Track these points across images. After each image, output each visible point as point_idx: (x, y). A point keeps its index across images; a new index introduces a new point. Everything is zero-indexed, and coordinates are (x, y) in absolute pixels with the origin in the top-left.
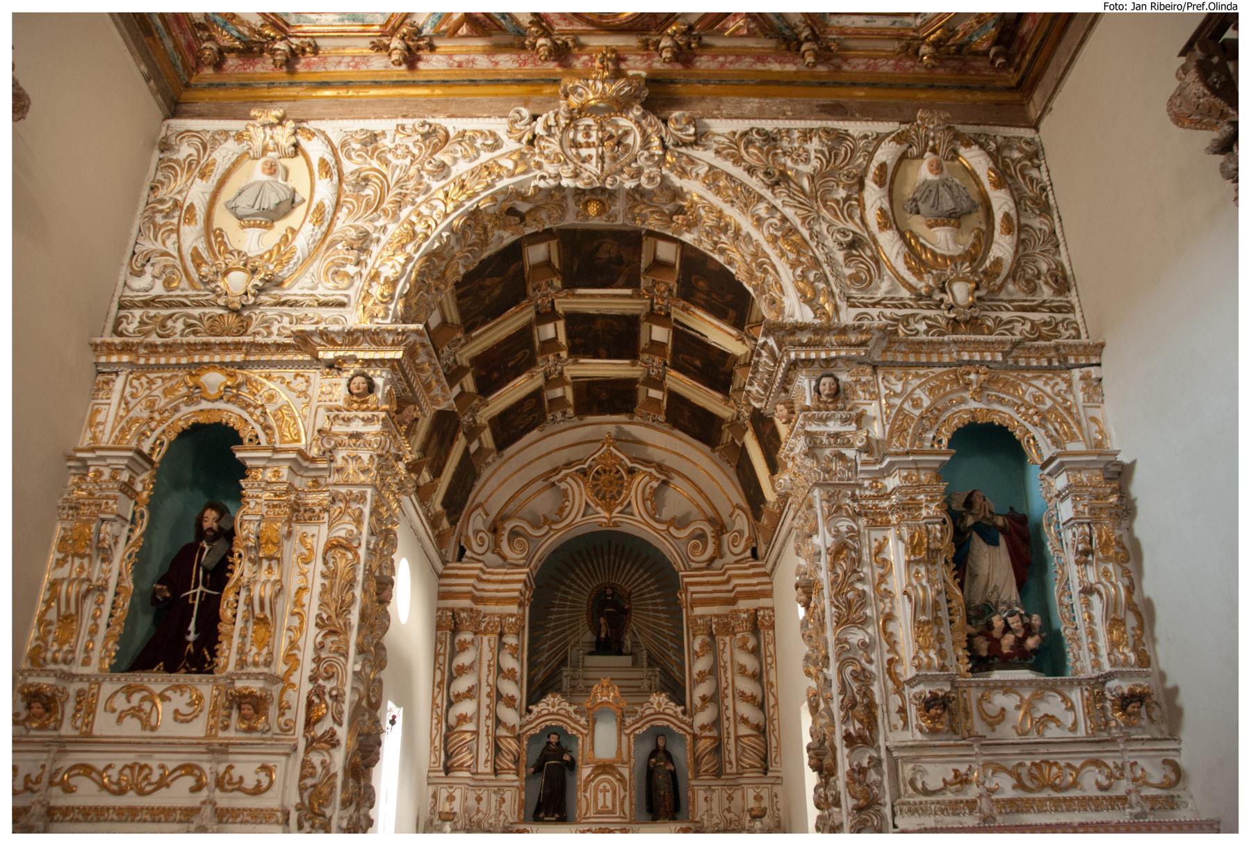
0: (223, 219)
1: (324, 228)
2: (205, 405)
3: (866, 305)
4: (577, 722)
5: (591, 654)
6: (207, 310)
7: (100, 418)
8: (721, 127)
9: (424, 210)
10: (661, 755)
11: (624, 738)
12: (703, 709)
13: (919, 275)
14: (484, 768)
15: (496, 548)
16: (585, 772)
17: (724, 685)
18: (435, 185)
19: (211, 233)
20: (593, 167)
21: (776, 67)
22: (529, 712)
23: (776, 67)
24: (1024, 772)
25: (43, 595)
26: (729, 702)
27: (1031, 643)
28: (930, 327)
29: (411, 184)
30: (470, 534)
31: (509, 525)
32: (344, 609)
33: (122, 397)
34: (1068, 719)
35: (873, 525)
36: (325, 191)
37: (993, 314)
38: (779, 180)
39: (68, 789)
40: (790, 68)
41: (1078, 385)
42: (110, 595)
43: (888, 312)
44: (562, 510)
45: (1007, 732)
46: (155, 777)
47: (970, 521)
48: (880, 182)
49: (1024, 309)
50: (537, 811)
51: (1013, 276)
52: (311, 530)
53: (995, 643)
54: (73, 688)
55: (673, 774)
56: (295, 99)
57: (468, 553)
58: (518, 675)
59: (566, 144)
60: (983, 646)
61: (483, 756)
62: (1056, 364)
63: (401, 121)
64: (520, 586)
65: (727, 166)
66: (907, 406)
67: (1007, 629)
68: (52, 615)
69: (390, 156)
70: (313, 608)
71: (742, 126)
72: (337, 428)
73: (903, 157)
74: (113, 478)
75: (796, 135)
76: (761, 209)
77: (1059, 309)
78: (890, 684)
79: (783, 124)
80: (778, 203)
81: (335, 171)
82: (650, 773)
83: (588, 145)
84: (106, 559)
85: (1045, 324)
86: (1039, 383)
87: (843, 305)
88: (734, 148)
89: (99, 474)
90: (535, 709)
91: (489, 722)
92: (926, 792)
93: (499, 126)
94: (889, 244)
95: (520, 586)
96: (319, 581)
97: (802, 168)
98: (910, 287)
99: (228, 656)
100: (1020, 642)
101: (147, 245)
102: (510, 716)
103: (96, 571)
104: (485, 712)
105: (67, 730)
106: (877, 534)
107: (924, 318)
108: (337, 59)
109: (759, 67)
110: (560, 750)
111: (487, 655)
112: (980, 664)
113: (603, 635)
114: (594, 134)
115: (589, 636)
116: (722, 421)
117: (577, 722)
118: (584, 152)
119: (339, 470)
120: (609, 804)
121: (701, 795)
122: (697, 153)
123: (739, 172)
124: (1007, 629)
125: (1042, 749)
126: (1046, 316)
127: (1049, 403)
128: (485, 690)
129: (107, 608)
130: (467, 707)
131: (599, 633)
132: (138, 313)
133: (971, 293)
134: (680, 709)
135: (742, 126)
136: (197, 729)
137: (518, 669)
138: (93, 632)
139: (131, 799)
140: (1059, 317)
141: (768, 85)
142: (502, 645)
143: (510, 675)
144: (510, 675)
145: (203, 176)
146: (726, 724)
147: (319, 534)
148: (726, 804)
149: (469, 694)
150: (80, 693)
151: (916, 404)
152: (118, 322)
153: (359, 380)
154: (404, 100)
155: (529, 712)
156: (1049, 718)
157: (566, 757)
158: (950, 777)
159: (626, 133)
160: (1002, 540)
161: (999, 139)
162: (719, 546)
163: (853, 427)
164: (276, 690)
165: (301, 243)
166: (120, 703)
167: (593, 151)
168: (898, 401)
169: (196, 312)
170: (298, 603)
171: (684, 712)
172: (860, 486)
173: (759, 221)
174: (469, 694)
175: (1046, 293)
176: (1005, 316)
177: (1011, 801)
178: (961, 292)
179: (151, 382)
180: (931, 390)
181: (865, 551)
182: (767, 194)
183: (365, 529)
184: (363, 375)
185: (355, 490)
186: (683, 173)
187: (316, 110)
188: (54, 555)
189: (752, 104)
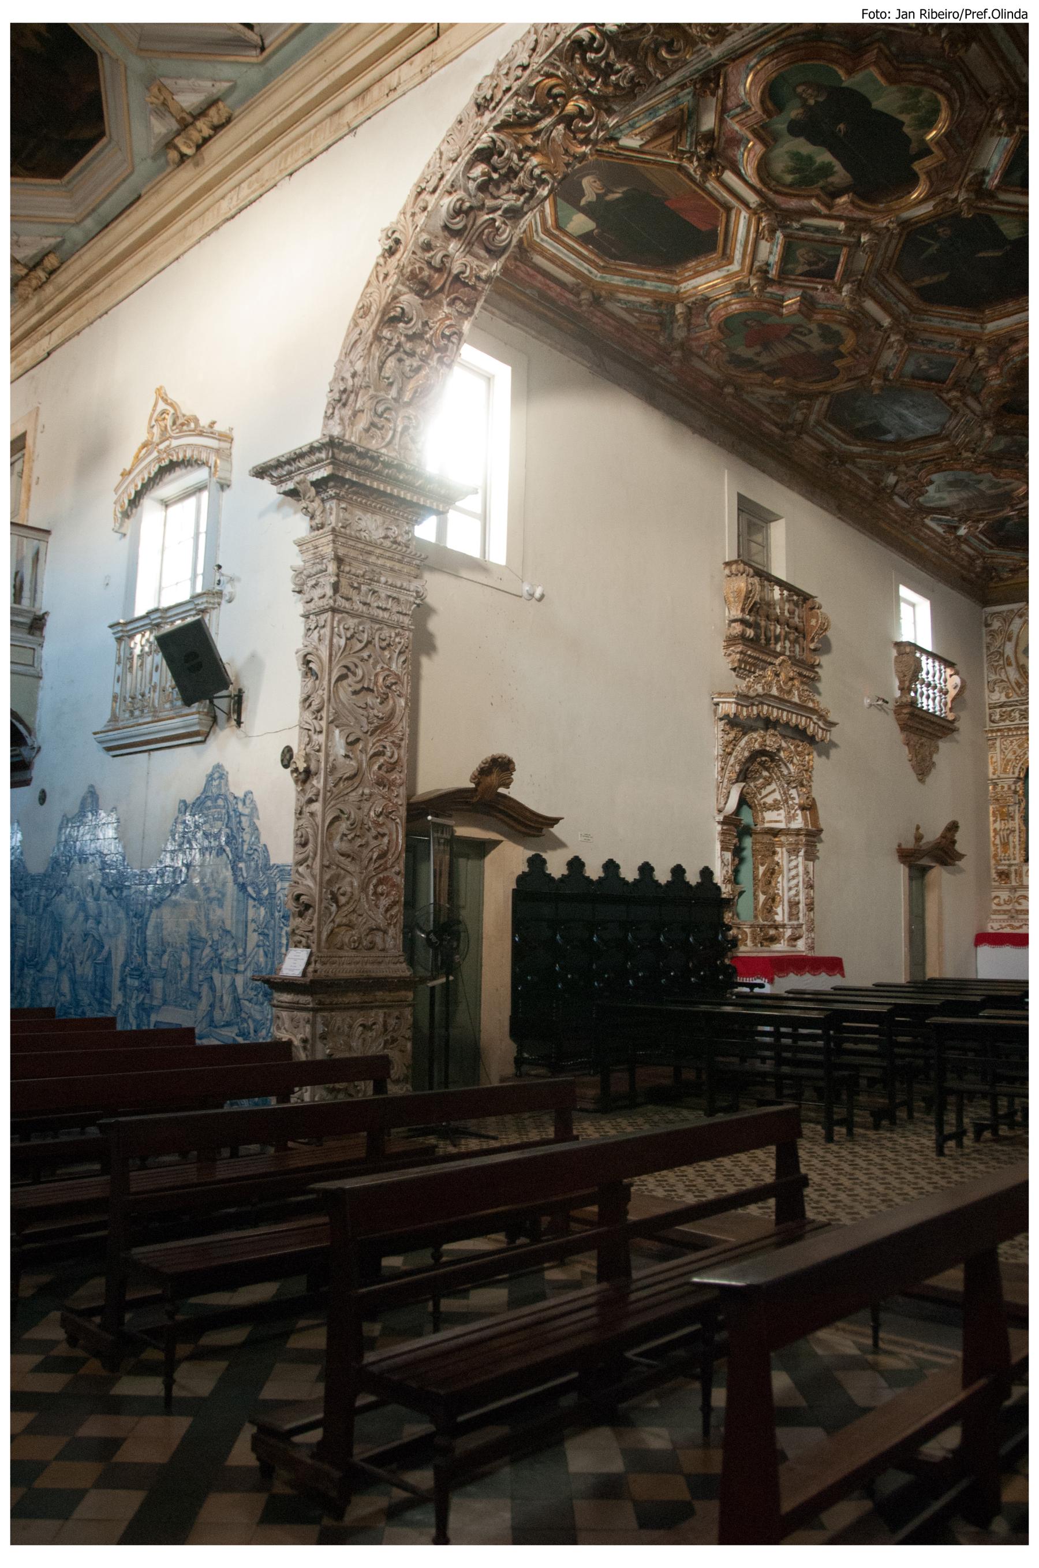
25: (992, 834)
39: (1020, 904)
54: (1013, 868)
68: (998, 841)
74: (1009, 788)
84: (1013, 820)
89: (1003, 787)
103: (1011, 824)
105: (1014, 884)
129: (1017, 838)
138: (1014, 847)
150: (1016, 871)
188: (992, 819)
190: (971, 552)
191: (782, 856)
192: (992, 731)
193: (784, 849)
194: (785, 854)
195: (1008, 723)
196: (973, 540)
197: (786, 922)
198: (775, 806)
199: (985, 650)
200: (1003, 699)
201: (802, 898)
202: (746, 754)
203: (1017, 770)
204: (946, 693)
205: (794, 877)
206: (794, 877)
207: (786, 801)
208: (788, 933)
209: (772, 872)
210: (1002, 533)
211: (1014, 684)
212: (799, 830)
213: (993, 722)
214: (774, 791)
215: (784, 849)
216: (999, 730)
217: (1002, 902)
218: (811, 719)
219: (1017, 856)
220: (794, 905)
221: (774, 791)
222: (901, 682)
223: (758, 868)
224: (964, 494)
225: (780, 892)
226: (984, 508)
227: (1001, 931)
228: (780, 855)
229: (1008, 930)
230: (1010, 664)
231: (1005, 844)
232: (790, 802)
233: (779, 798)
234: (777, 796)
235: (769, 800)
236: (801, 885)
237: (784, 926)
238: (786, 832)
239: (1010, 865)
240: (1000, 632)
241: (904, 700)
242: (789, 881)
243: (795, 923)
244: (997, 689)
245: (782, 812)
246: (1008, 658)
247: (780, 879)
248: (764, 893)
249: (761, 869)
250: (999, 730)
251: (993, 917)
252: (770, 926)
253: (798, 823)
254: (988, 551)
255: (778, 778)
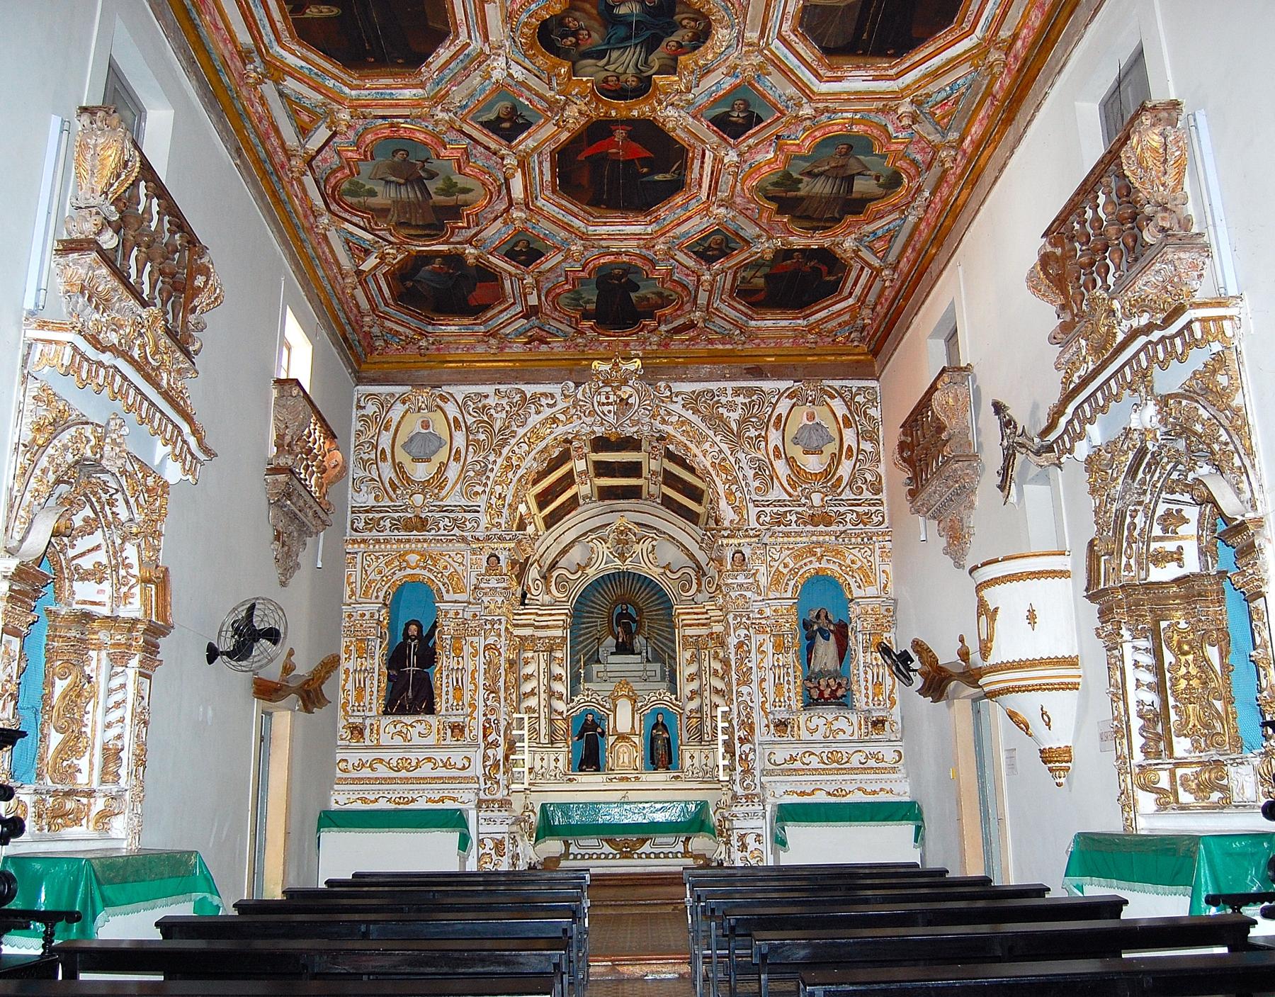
0: (402, 456)
1: (462, 463)
2: (409, 571)
3: (764, 506)
4: (604, 707)
5: (612, 654)
6: (402, 514)
7: (352, 579)
8: (687, 387)
9: (516, 448)
10: (660, 727)
11: (637, 717)
12: (691, 699)
13: (794, 488)
14: (545, 740)
15: (548, 592)
16: (611, 739)
17: (704, 682)
18: (521, 432)
19: (398, 467)
20: (611, 418)
21: (721, 347)
22: (572, 701)
23: (721, 347)
24: (824, 755)
26: (707, 694)
27: (839, 693)
28: (799, 518)
29: (507, 432)
30: (530, 583)
31: (555, 574)
32: (495, 680)
33: (363, 567)
34: (849, 730)
35: (758, 632)
36: (460, 440)
37: (835, 509)
38: (718, 423)
40: (729, 347)
41: (878, 552)
42: (376, 675)
43: (775, 509)
44: (591, 559)
45: (818, 736)
46: (414, 763)
47: (816, 627)
48: (777, 425)
49: (853, 505)
50: (581, 765)
51: (850, 484)
52: (475, 639)
53: (821, 694)
54: (368, 722)
55: (668, 740)
56: (431, 368)
57: (529, 596)
58: (564, 678)
59: (596, 404)
60: (815, 694)
61: (543, 732)
62: (866, 540)
63: (497, 387)
64: (563, 617)
65: (689, 414)
66: (781, 568)
67: (828, 685)
69: (492, 411)
70: (481, 681)
71: (699, 387)
72: (482, 585)
73: (794, 405)
74: (372, 615)
75: (729, 392)
76: (707, 446)
77: (874, 505)
78: (762, 713)
79: (722, 384)
80: (718, 439)
81: (463, 425)
82: (653, 740)
83: (608, 404)
84: (373, 658)
85: (866, 514)
86: (855, 551)
87: (751, 505)
88: (692, 402)
90: (576, 699)
91: (546, 710)
92: (775, 764)
93: (555, 389)
94: (781, 468)
95: (563, 617)
96: (482, 666)
97: (731, 414)
98: (790, 495)
99: (440, 705)
100: (833, 692)
101: (362, 474)
102: (560, 706)
103: (367, 664)
104: (543, 703)
106: (761, 637)
107: (796, 513)
108: (455, 346)
109: (710, 347)
110: (594, 725)
111: (543, 665)
112: (811, 702)
113: (620, 640)
114: (611, 397)
115: (610, 641)
116: (698, 515)
117: (604, 707)
118: (606, 408)
119: (486, 608)
120: (626, 760)
121: (687, 755)
122: (671, 407)
123: (695, 419)
124: (828, 685)
125: (834, 745)
126: (866, 509)
127: (859, 564)
128: (543, 688)
129: (376, 683)
130: (532, 702)
131: (617, 639)
132: (363, 516)
133: (822, 500)
134: (673, 697)
135: (699, 387)
136: (432, 739)
137: (564, 674)
139: (403, 774)
140: (873, 509)
141: (714, 357)
142: (551, 659)
143: (558, 678)
144: (558, 678)
145: (387, 429)
146: (705, 709)
147: (480, 642)
148: (704, 761)
149: (532, 693)
151: (786, 566)
152: (353, 523)
153: (493, 559)
154: (498, 370)
155: (572, 701)
156: (842, 730)
157: (599, 730)
158: (788, 759)
159: (631, 396)
160: (832, 637)
161: (854, 390)
162: (699, 584)
163: (751, 580)
164: (467, 720)
165: (453, 471)
166: (391, 729)
167: (611, 408)
168: (776, 564)
169: (396, 515)
170: (473, 678)
171: (676, 699)
172: (752, 611)
173: (705, 453)
174: (532, 693)
175: (867, 495)
176: (842, 509)
177: (816, 770)
178: (816, 499)
179: (377, 558)
180: (795, 557)
181: (754, 646)
182: (711, 433)
183: (503, 639)
184: (495, 556)
185: (496, 618)
186: (664, 422)
187: (444, 377)
189: (707, 368)
190: (365, 305)
191: (98, 663)
192: (354, 541)
193: (104, 653)
194: (105, 662)
195: (374, 532)
196: (372, 285)
197: (95, 785)
198: (96, 574)
199: (353, 439)
200: (371, 502)
201: (128, 741)
202: (70, 458)
203: (382, 594)
204: (324, 471)
205: (117, 705)
206: (117, 705)
207: (115, 569)
208: (99, 804)
209: (77, 696)
210: (409, 284)
211: (387, 486)
212: (135, 621)
213: (356, 530)
214: (98, 547)
215: (104, 653)
216: (364, 541)
217: (350, 767)
218: (180, 432)
219: (374, 709)
220: (111, 755)
221: (98, 547)
222: (280, 437)
223: (53, 684)
224: (408, 194)
225: (88, 730)
226: (417, 227)
227: (349, 807)
228: (94, 664)
229: (359, 806)
230: (384, 459)
231: (360, 690)
232: (122, 572)
233: (105, 561)
234: (101, 557)
235: (87, 563)
236: (128, 720)
237: (90, 794)
238: (112, 621)
239: (365, 718)
240: (375, 418)
241: (282, 461)
242: (108, 710)
243: (114, 788)
244: (364, 489)
245: (106, 585)
246: (383, 451)
247: (90, 708)
248: (59, 730)
249: (60, 686)
250: (364, 541)
251: (336, 787)
252: (69, 794)
253: (133, 609)
254: (382, 307)
255: (108, 527)
